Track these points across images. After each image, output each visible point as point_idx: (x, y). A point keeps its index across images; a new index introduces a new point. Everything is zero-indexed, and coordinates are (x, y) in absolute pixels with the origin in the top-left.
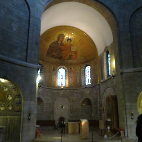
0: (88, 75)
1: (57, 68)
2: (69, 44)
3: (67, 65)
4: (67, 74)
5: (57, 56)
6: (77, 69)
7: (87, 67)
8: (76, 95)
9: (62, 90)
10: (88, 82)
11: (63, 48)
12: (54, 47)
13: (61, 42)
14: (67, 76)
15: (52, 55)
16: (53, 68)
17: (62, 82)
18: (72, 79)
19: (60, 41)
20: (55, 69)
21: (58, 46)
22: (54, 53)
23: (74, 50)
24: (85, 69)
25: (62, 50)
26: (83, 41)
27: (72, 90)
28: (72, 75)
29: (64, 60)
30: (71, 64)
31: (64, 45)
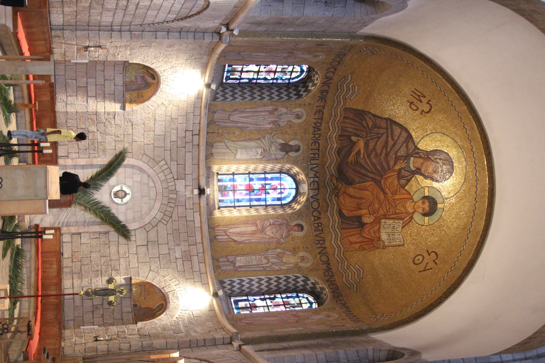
0: (278, 305)
1: (295, 162)
2: (410, 210)
3: (315, 210)
4: (271, 212)
5: (351, 158)
6: (301, 254)
7: (311, 299)
8: (178, 254)
9: (196, 192)
10: (241, 304)
11: (392, 180)
12: (391, 142)
13: (418, 171)
14: (262, 212)
15: (354, 138)
16: (292, 143)
17: (234, 191)
18: (253, 233)
19: (418, 165)
20: (292, 154)
21: (397, 159)
22: (361, 144)
23: (384, 237)
24: (304, 291)
25: (378, 183)
26: (432, 264)
27: (199, 240)
28: (269, 232)
29: (336, 192)
30: (319, 228)
31: (403, 187)
